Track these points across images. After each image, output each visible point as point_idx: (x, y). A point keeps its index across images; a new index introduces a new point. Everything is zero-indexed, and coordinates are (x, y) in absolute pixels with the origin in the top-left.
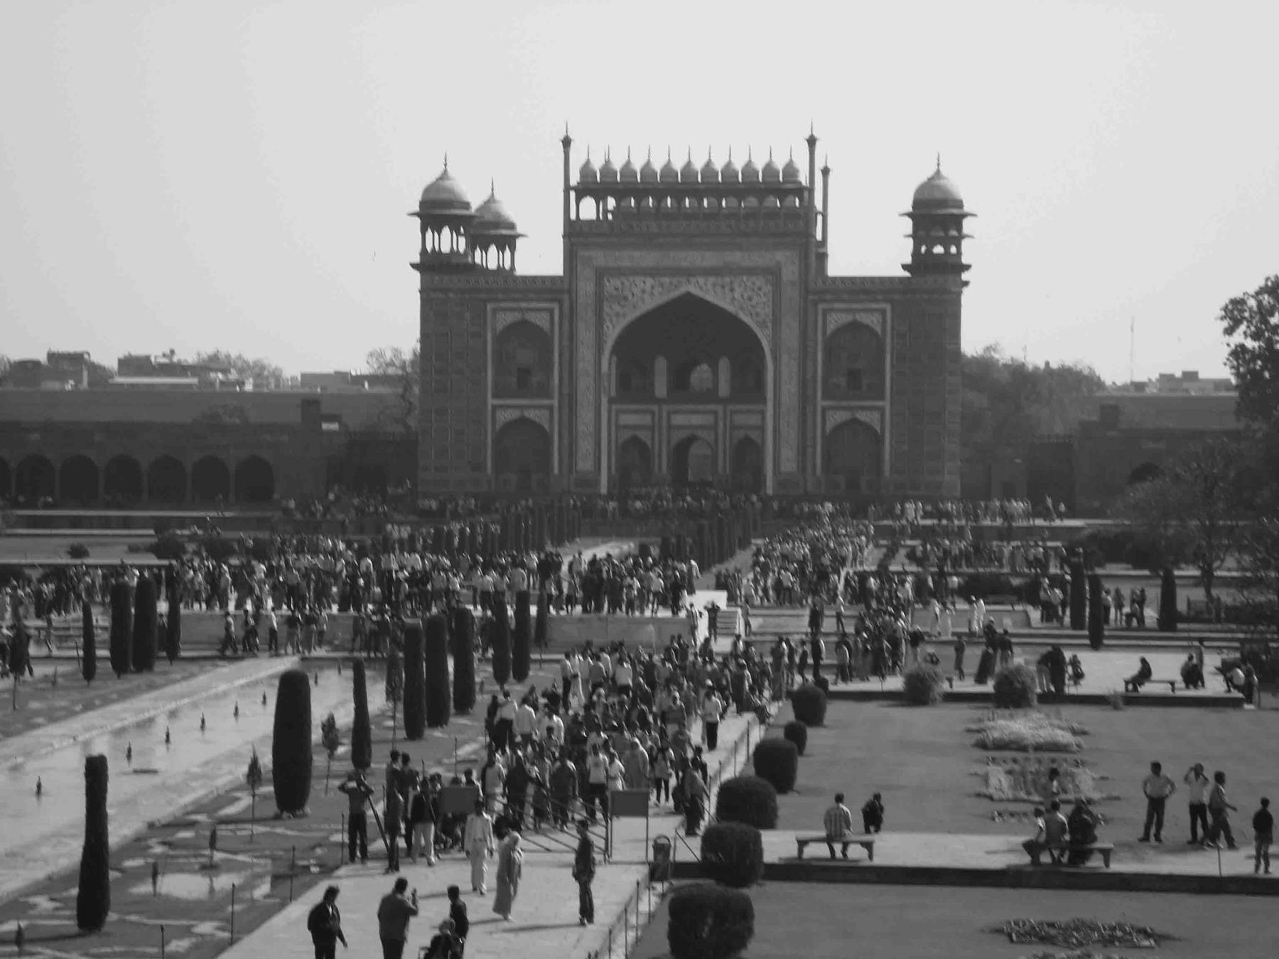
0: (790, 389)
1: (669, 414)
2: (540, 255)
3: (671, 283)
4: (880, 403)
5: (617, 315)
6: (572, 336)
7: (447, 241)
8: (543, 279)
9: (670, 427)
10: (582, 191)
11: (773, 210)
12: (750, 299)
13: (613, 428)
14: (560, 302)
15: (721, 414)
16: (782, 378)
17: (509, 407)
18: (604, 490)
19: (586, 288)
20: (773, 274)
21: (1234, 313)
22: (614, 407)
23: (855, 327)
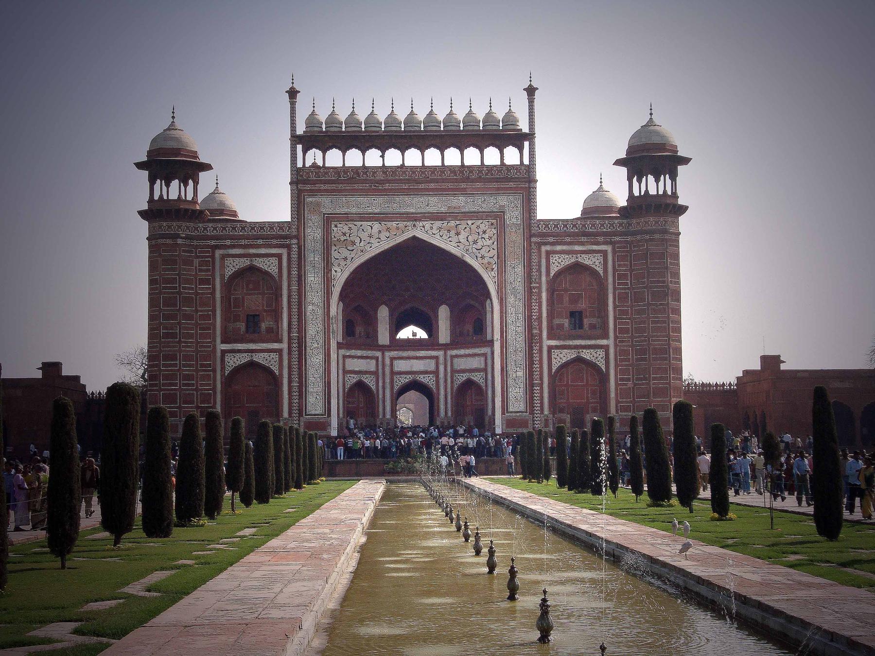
1: (392, 359)
3: (398, 228)
4: (604, 342)
5: (345, 259)
6: (301, 279)
8: (271, 225)
9: (393, 373)
12: (475, 242)
13: (341, 371)
14: (288, 247)
15: (441, 359)
16: (507, 316)
17: (239, 351)
18: (334, 433)
19: (313, 233)
20: (498, 217)
22: (342, 352)
23: (577, 268)
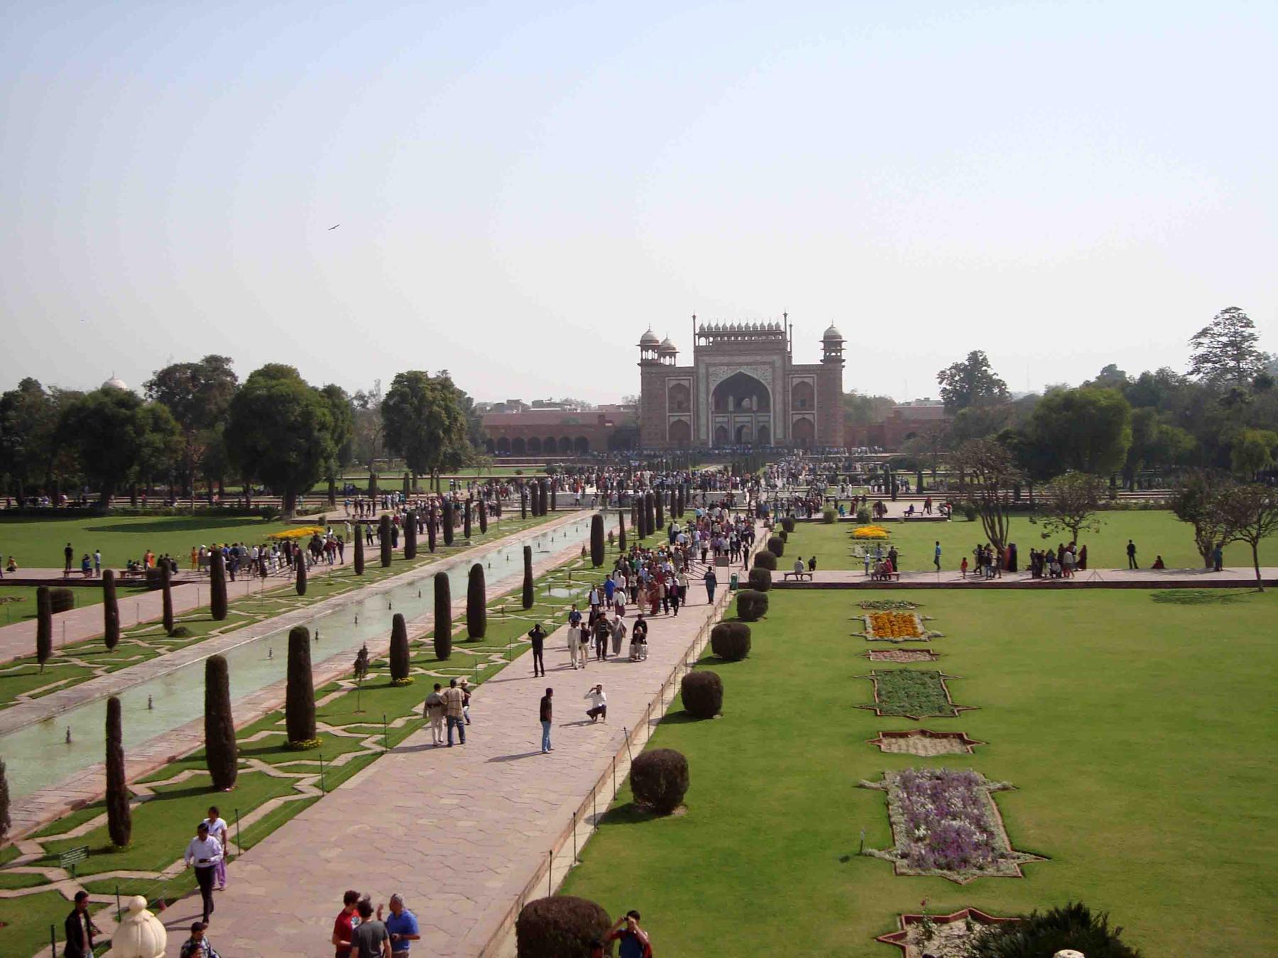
0: (779, 407)
2: (685, 359)
7: (650, 355)
10: (700, 335)
11: (771, 341)
16: (776, 402)
19: (702, 371)
20: (772, 364)
21: (942, 376)
